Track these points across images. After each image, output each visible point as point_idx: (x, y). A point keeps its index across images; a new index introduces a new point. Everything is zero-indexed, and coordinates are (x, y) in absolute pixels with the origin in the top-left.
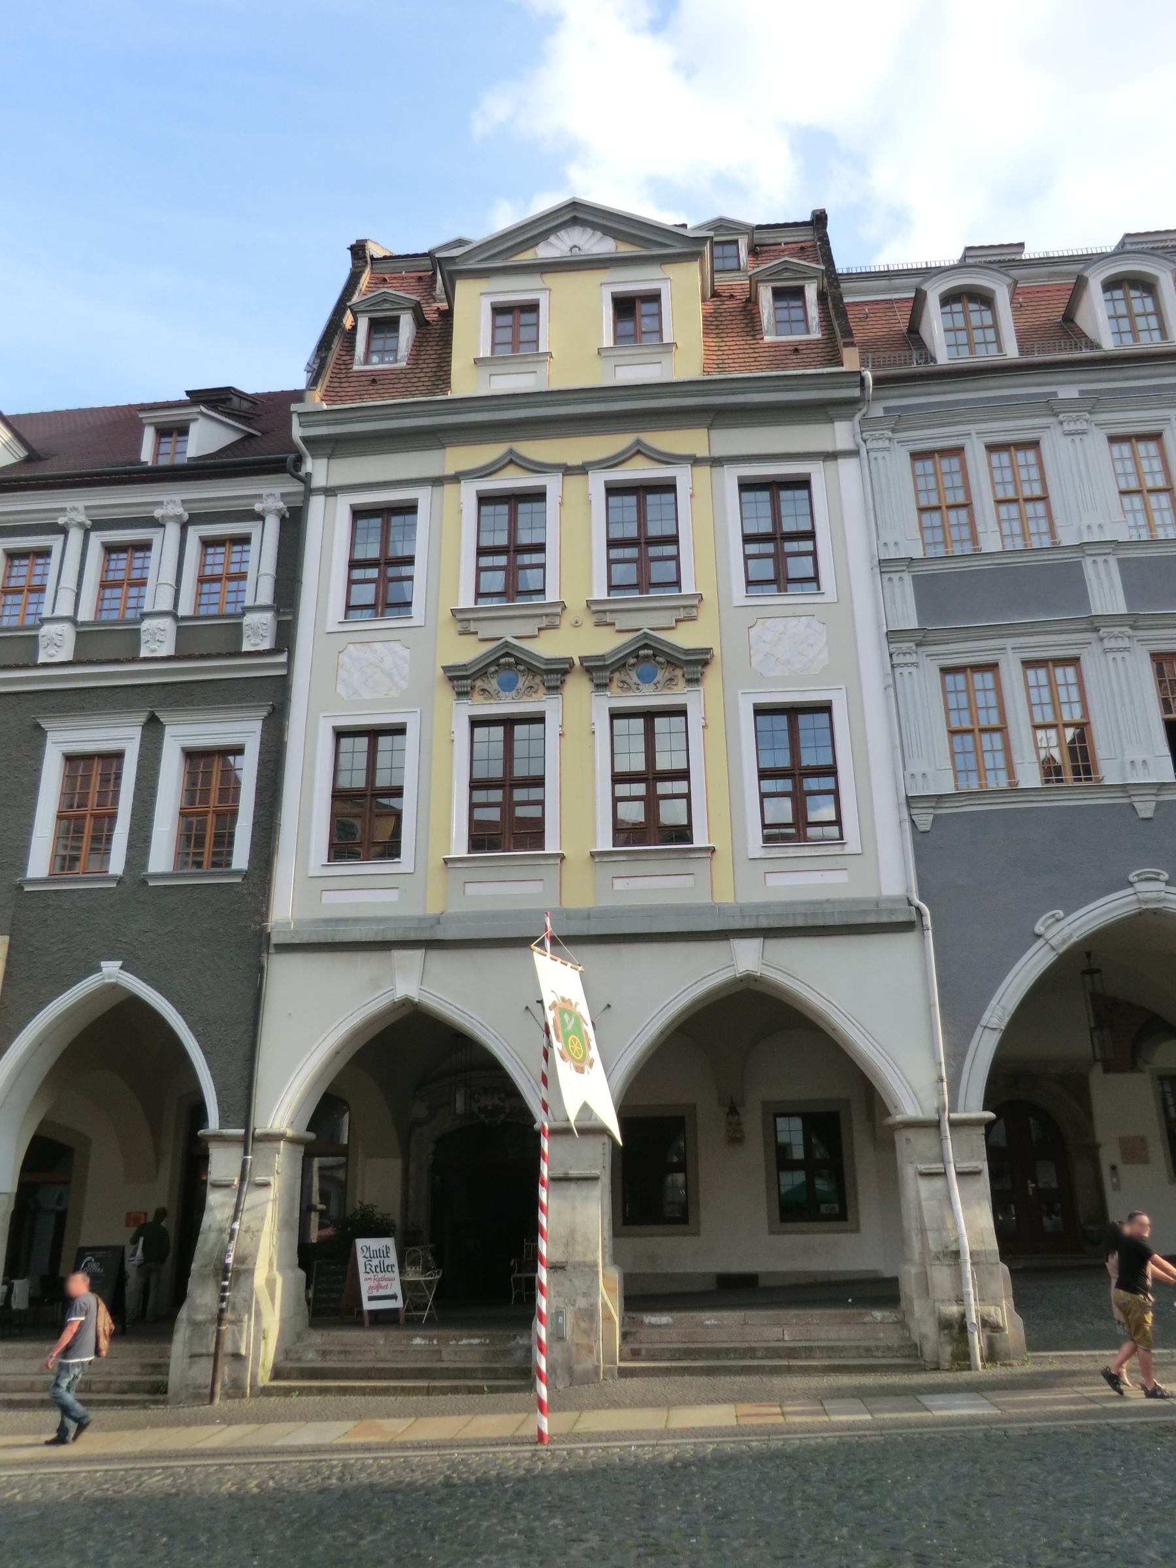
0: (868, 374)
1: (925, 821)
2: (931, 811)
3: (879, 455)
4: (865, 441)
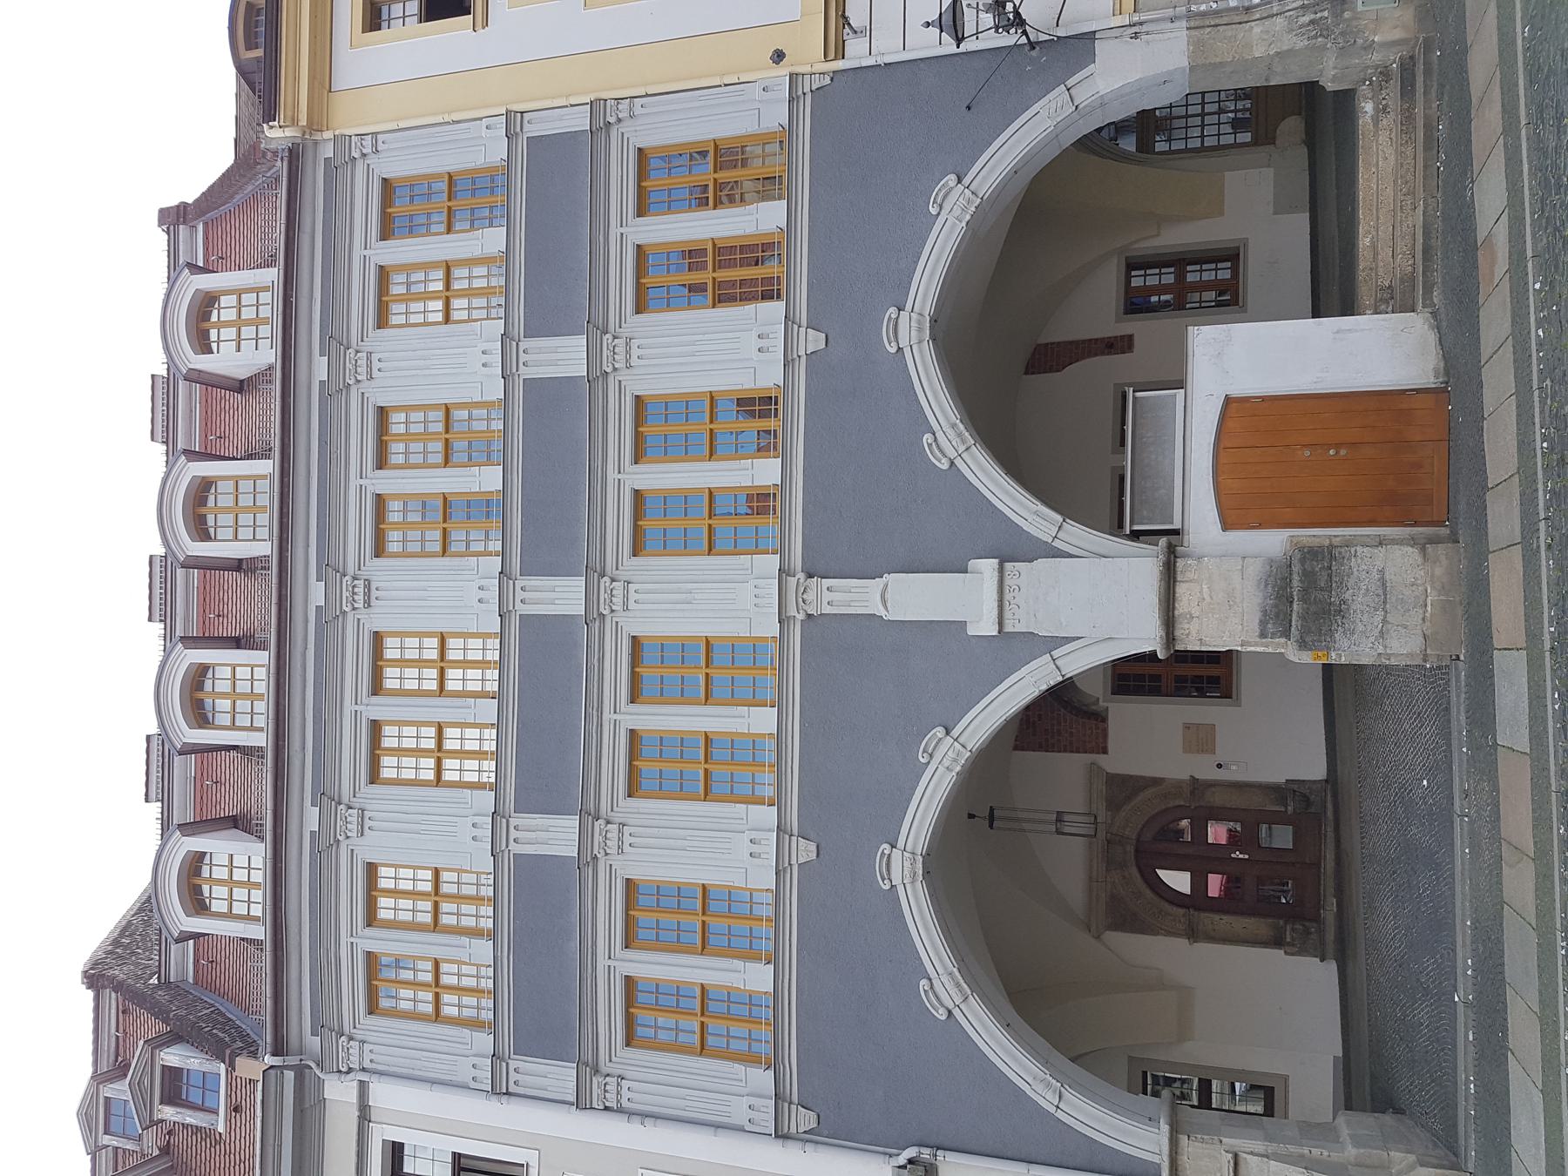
0: (269, 1060)
1: (805, 1120)
2: (793, 1107)
3: (367, 1057)
4: (350, 1070)
